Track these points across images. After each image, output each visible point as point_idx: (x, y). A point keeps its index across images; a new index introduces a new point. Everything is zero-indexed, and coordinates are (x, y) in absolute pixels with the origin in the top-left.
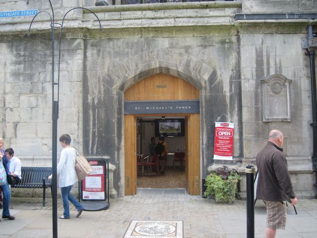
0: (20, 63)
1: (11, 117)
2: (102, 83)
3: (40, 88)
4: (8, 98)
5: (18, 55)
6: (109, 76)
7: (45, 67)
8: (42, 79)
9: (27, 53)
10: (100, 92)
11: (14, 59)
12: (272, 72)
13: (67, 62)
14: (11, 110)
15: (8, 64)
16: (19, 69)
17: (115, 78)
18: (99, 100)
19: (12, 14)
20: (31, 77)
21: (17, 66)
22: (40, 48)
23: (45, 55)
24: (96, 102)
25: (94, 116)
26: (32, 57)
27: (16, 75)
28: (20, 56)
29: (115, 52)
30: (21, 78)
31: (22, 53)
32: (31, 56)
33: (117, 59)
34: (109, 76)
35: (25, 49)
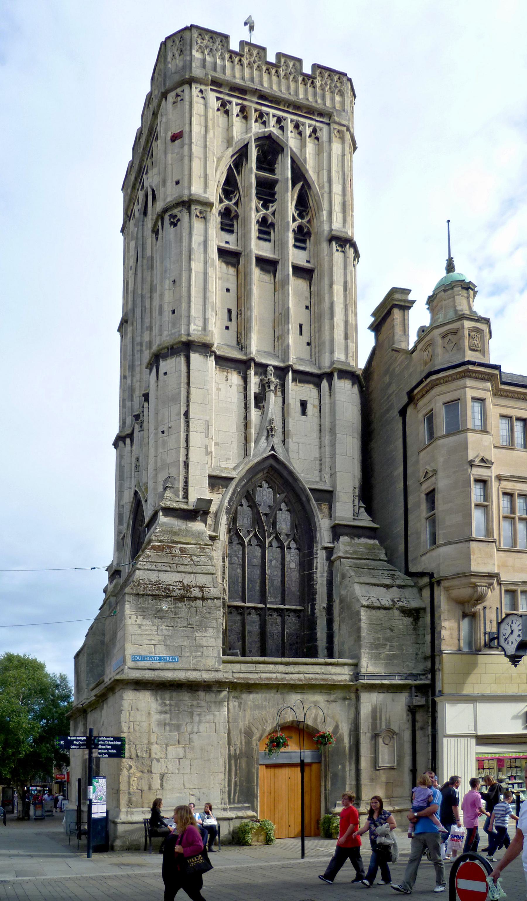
0: (165, 713)
1: (157, 769)
2: (243, 735)
3: (187, 739)
4: (155, 748)
6: (249, 728)
7: (192, 717)
8: (189, 730)
9: (173, 703)
10: (241, 744)
11: (159, 708)
12: (384, 727)
13: (214, 714)
14: (158, 761)
15: (152, 713)
16: (165, 719)
17: (254, 729)
18: (241, 750)
19: (151, 659)
20: (178, 727)
21: (163, 716)
22: (186, 697)
23: (192, 705)
24: (238, 752)
25: (236, 766)
26: (179, 708)
27: (163, 724)
28: (166, 705)
29: (255, 705)
30: (168, 728)
31: (168, 702)
32: (177, 705)
33: (257, 712)
34: (249, 728)
35: (171, 699)
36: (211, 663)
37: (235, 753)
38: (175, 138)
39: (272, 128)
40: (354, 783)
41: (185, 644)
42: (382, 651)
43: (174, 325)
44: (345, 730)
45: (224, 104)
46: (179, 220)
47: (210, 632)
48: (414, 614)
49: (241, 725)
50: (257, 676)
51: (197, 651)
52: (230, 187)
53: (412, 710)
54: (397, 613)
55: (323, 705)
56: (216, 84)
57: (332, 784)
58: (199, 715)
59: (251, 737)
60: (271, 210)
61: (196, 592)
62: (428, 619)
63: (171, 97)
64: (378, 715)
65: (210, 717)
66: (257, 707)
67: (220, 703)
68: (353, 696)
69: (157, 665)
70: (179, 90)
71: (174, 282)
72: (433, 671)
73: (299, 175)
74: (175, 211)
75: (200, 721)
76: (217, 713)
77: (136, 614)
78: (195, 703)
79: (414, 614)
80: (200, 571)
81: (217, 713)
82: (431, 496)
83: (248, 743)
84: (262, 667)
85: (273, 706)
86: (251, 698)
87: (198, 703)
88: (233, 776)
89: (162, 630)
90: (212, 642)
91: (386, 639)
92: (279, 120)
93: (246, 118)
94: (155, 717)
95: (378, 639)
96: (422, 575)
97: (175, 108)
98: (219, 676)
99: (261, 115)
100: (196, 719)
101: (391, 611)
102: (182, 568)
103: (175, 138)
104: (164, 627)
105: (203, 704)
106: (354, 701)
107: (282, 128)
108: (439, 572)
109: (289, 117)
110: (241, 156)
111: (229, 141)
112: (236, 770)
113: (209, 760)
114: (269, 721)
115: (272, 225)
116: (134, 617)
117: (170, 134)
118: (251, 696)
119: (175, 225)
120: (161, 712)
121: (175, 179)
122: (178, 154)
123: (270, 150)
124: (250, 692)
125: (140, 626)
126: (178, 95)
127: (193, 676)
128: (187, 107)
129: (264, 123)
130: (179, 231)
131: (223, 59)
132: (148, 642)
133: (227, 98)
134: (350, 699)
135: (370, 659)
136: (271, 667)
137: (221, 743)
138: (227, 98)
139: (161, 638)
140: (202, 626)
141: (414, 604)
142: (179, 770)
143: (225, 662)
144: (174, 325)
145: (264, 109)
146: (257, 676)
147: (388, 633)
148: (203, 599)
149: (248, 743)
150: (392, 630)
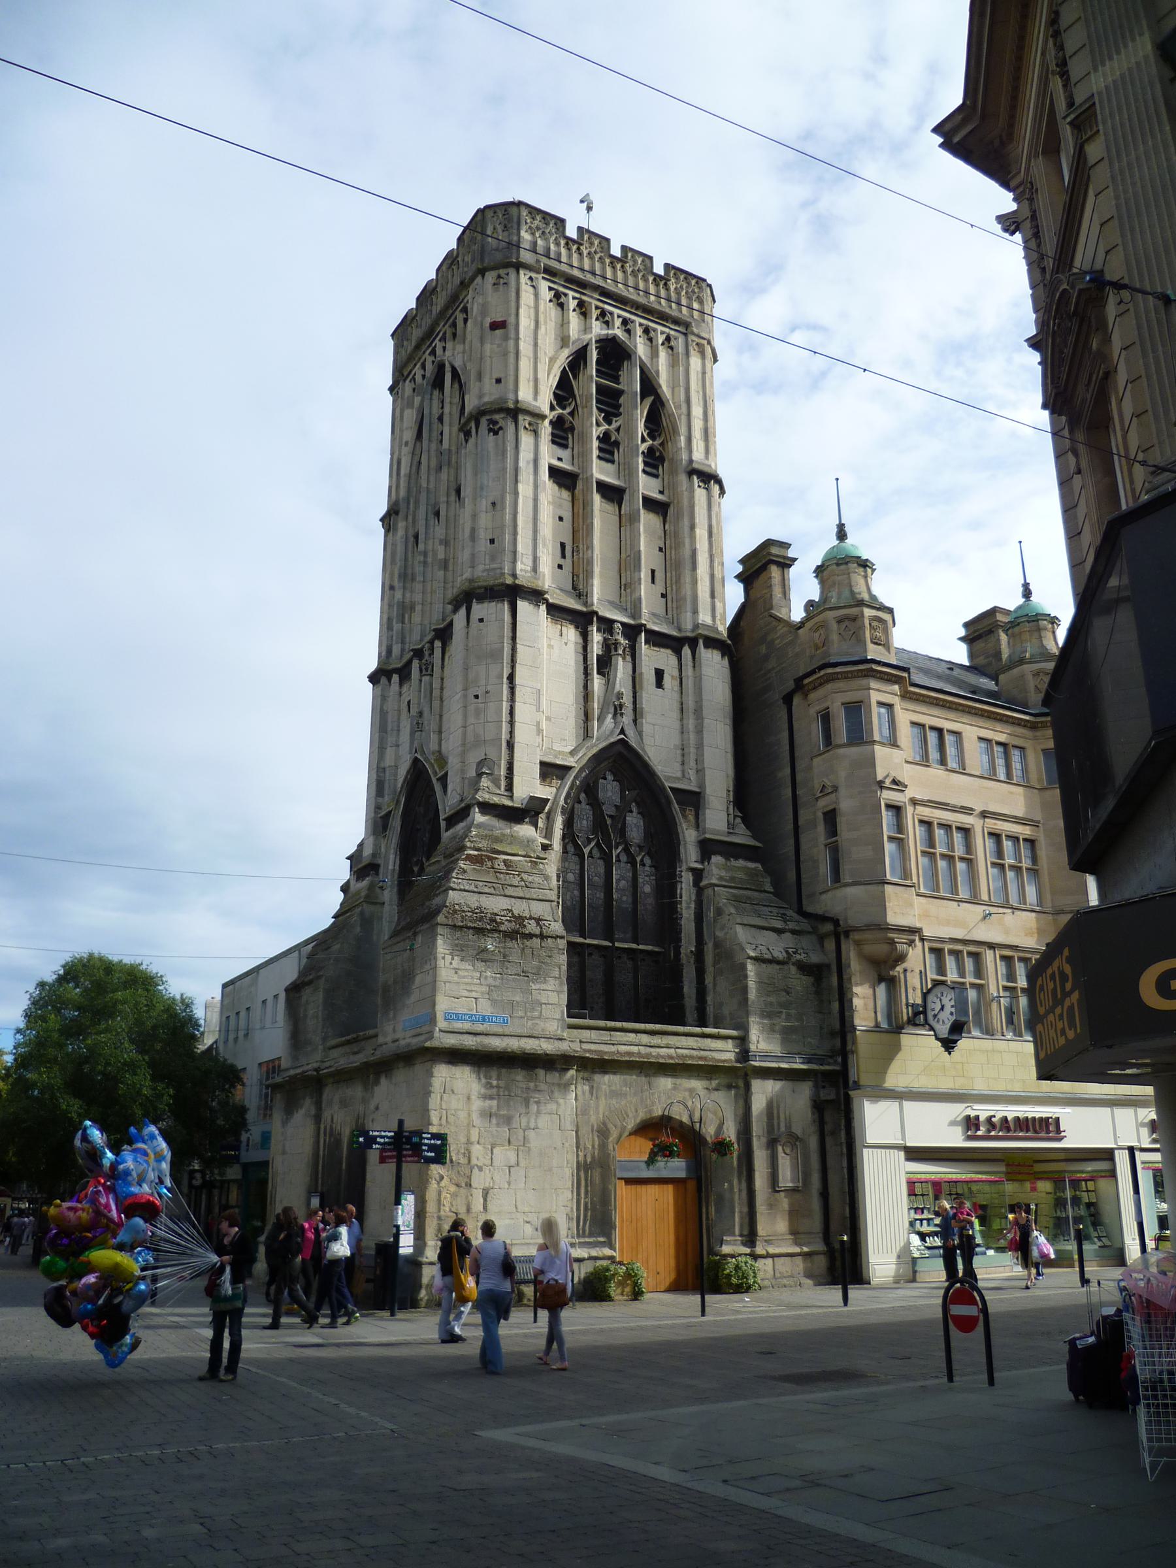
0: (491, 1098)
1: (479, 1180)
2: (596, 1134)
3: (521, 1138)
4: (477, 1150)
5: (489, 1086)
6: (604, 1124)
7: (527, 1106)
8: (524, 1124)
9: (502, 1083)
10: (593, 1147)
11: (483, 1091)
12: (783, 1129)
13: (557, 1103)
14: (480, 1169)
15: (473, 1097)
16: (491, 1107)
17: (610, 1126)
18: (593, 1157)
19: (471, 1018)
20: (508, 1120)
21: (488, 1102)
22: (519, 1076)
23: (528, 1088)
24: (589, 1160)
25: (586, 1180)
26: (509, 1091)
27: (488, 1115)
28: (492, 1087)
29: (612, 1091)
30: (494, 1121)
31: (495, 1083)
32: (507, 1088)
33: (614, 1102)
34: (604, 1124)
35: (498, 1079)
36: (553, 1027)
37: (585, 1161)
38: (495, 326)
39: (618, 331)
40: (745, 1210)
41: (517, 998)
42: (776, 1021)
44: (731, 1132)
45: (557, 295)
46: (501, 428)
47: (552, 984)
48: (815, 972)
49: (593, 1119)
50: (613, 1049)
51: (533, 1009)
52: (564, 392)
53: (819, 1106)
54: (793, 969)
55: (702, 1093)
56: (550, 272)
57: (717, 1211)
58: (538, 1103)
59: (607, 1138)
60: (614, 425)
61: (532, 927)
62: (834, 980)
63: (491, 277)
64: (775, 1112)
65: (552, 1107)
66: (614, 1094)
67: (565, 1087)
68: (741, 1084)
69: (479, 1027)
70: (502, 272)
73: (649, 387)
74: (497, 417)
75: (538, 1112)
76: (561, 1101)
77: (451, 954)
78: (532, 1085)
79: (815, 972)
80: (535, 897)
81: (561, 1101)
82: (831, 817)
83: (603, 1146)
84: (618, 1036)
85: (635, 1094)
86: (607, 1081)
87: (536, 1086)
88: (583, 1195)
89: (486, 977)
90: (553, 998)
91: (781, 1005)
92: (625, 322)
94: (477, 1104)
95: (771, 1004)
96: (824, 919)
97: (497, 290)
98: (564, 1047)
99: (603, 314)
100: (534, 1108)
101: (786, 967)
102: (510, 891)
103: (495, 326)
104: (489, 974)
105: (543, 1086)
106: (742, 1091)
107: (628, 331)
108: (846, 920)
109: (638, 320)
110: (578, 359)
111: (564, 341)
112: (586, 1186)
113: (550, 1170)
114: (631, 1115)
115: (617, 444)
116: (449, 958)
117: (488, 321)
118: (607, 1078)
119: (496, 433)
120: (485, 1097)
121: (496, 376)
122: (499, 346)
123: (614, 354)
124: (605, 1072)
126: (499, 277)
127: (530, 1045)
128: (513, 294)
129: (607, 323)
130: (500, 442)
131: (558, 244)
132: (467, 994)
133: (561, 289)
134: (736, 1087)
135: (762, 1031)
136: (631, 1037)
137: (567, 1145)
138: (561, 289)
139: (485, 989)
140: (540, 974)
141: (815, 958)
142: (509, 1183)
143: (571, 1027)
145: (607, 307)
146: (613, 1049)
147: (783, 997)
148: (542, 937)
149: (603, 1146)
150: (788, 993)
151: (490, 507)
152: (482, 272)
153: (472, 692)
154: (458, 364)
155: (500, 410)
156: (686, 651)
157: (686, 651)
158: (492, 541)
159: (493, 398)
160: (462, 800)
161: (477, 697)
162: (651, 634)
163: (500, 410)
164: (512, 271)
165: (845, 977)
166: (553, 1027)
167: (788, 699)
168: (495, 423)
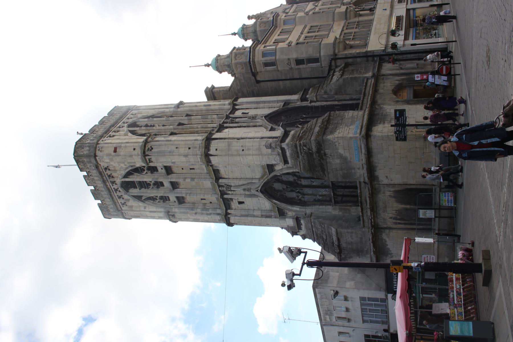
5: (380, 123)
38: (115, 151)
43: (196, 148)
45: (110, 136)
56: (101, 137)
63: (98, 153)
71: (177, 148)
72: (373, 56)
74: (147, 148)
79: (347, 65)
92: (124, 123)
93: (118, 131)
96: (330, 66)
97: (103, 151)
99: (119, 127)
105: (381, 112)
110: (133, 133)
111: (126, 135)
117: (113, 154)
119: (152, 149)
120: (384, 123)
121: (132, 150)
125: (339, 133)
126: (99, 150)
130: (156, 147)
139: (346, 127)
144: (196, 148)
145: (118, 126)
151: (178, 149)
152: (95, 156)
153: (241, 152)
154: (124, 173)
155: (145, 146)
156: (237, 107)
157: (237, 107)
158: (189, 148)
159: (140, 151)
160: (279, 155)
161: (243, 150)
162: (230, 114)
163: (145, 146)
164: (98, 146)
165: (350, 56)
166: (361, 113)
167: (258, 82)
168: (149, 149)
